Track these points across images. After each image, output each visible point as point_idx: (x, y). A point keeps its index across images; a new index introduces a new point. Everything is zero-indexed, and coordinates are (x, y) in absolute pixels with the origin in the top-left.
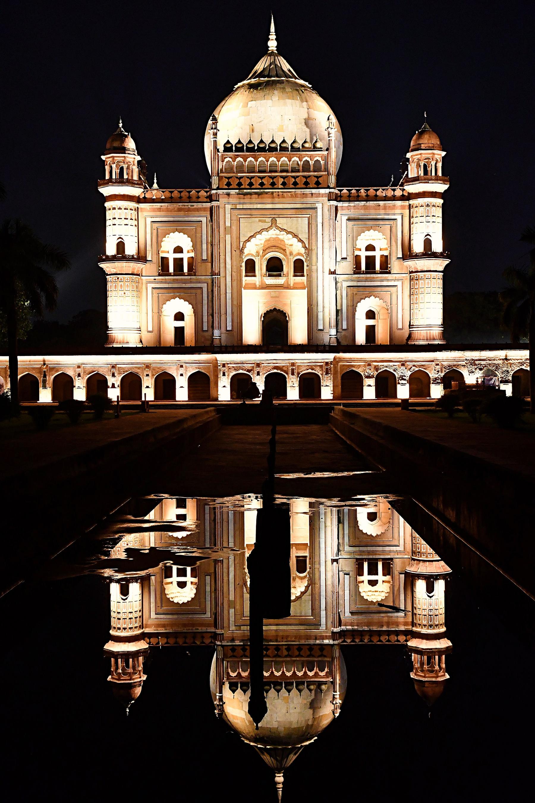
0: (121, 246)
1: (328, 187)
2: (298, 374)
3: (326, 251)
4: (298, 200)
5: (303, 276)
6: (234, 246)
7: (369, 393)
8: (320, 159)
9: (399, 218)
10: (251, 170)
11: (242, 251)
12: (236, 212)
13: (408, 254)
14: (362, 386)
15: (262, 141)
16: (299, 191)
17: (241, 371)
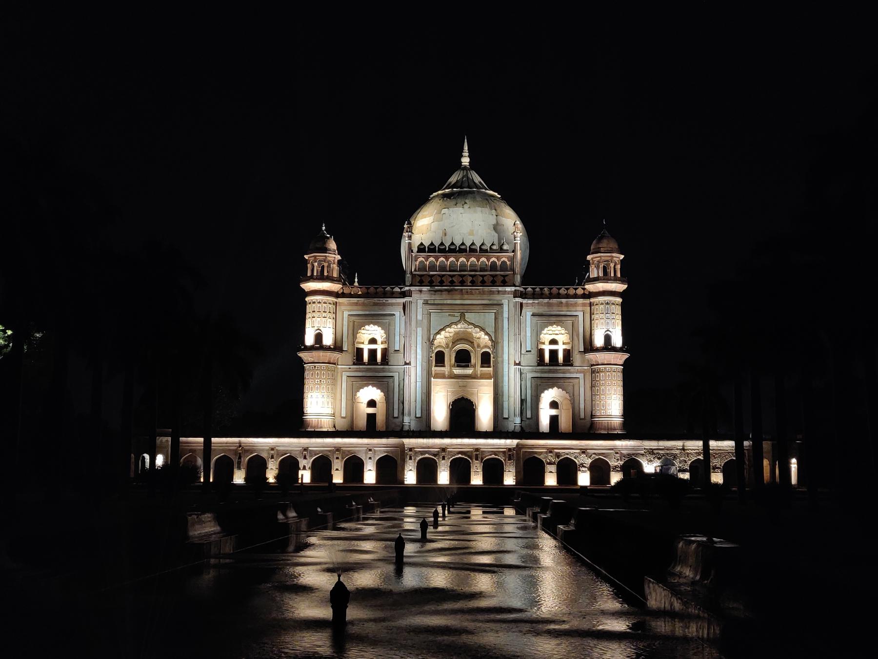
0: (319, 337)
1: (515, 286)
2: (482, 459)
3: (512, 344)
4: (485, 297)
5: (489, 367)
6: (425, 338)
8: (506, 260)
9: (580, 314)
10: (443, 268)
11: (431, 343)
12: (428, 307)
14: (544, 472)
15: (452, 244)
16: (486, 289)
17: (427, 455)
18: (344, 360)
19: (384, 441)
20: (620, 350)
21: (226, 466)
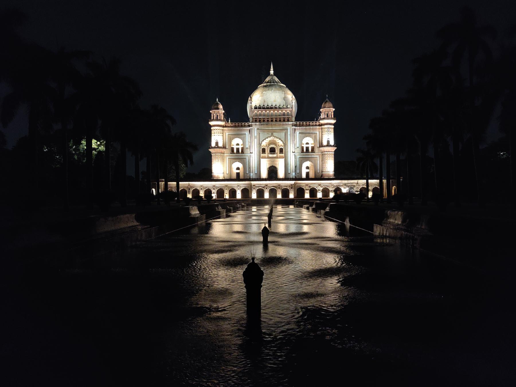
0: (217, 143)
3: (291, 145)
7: (307, 196)
9: (318, 132)
11: (260, 144)
12: (259, 131)
13: (321, 145)
18: (227, 152)
19: (244, 182)
20: (333, 146)
21: (184, 192)
